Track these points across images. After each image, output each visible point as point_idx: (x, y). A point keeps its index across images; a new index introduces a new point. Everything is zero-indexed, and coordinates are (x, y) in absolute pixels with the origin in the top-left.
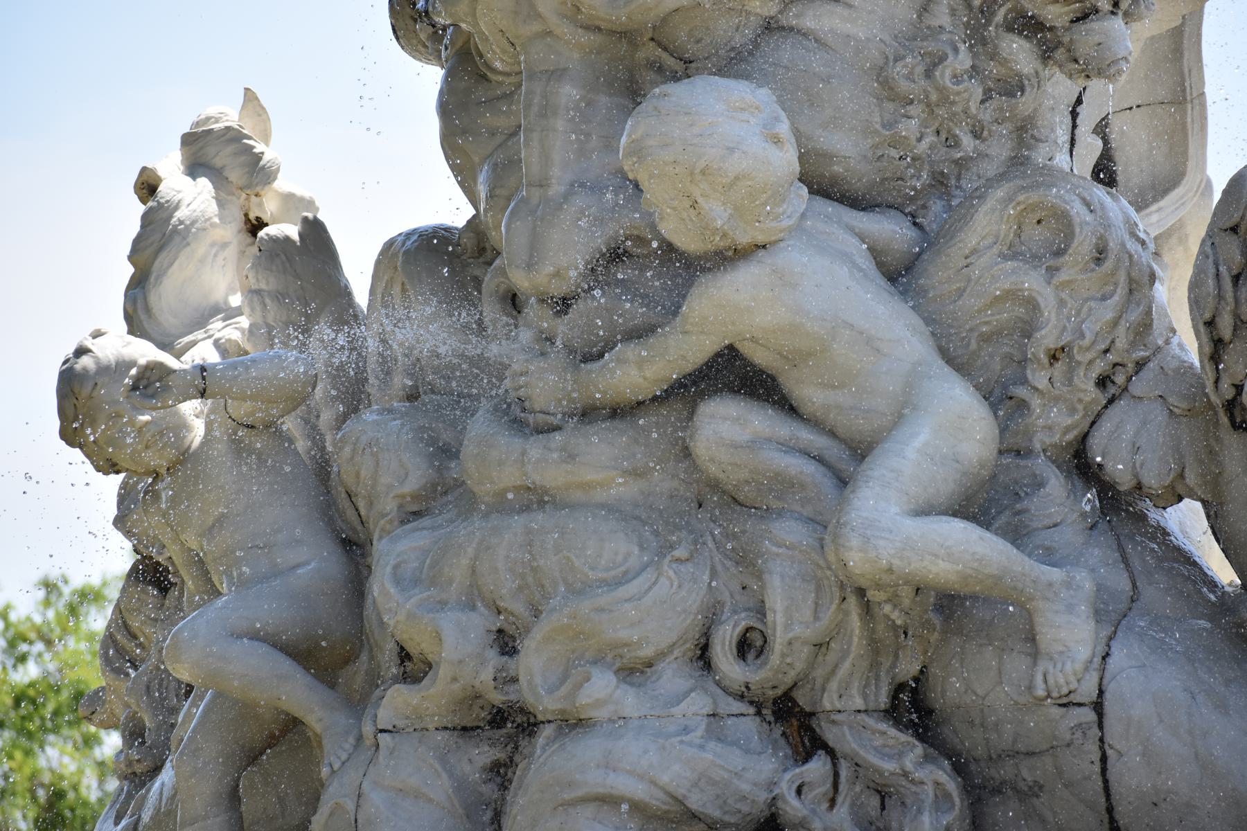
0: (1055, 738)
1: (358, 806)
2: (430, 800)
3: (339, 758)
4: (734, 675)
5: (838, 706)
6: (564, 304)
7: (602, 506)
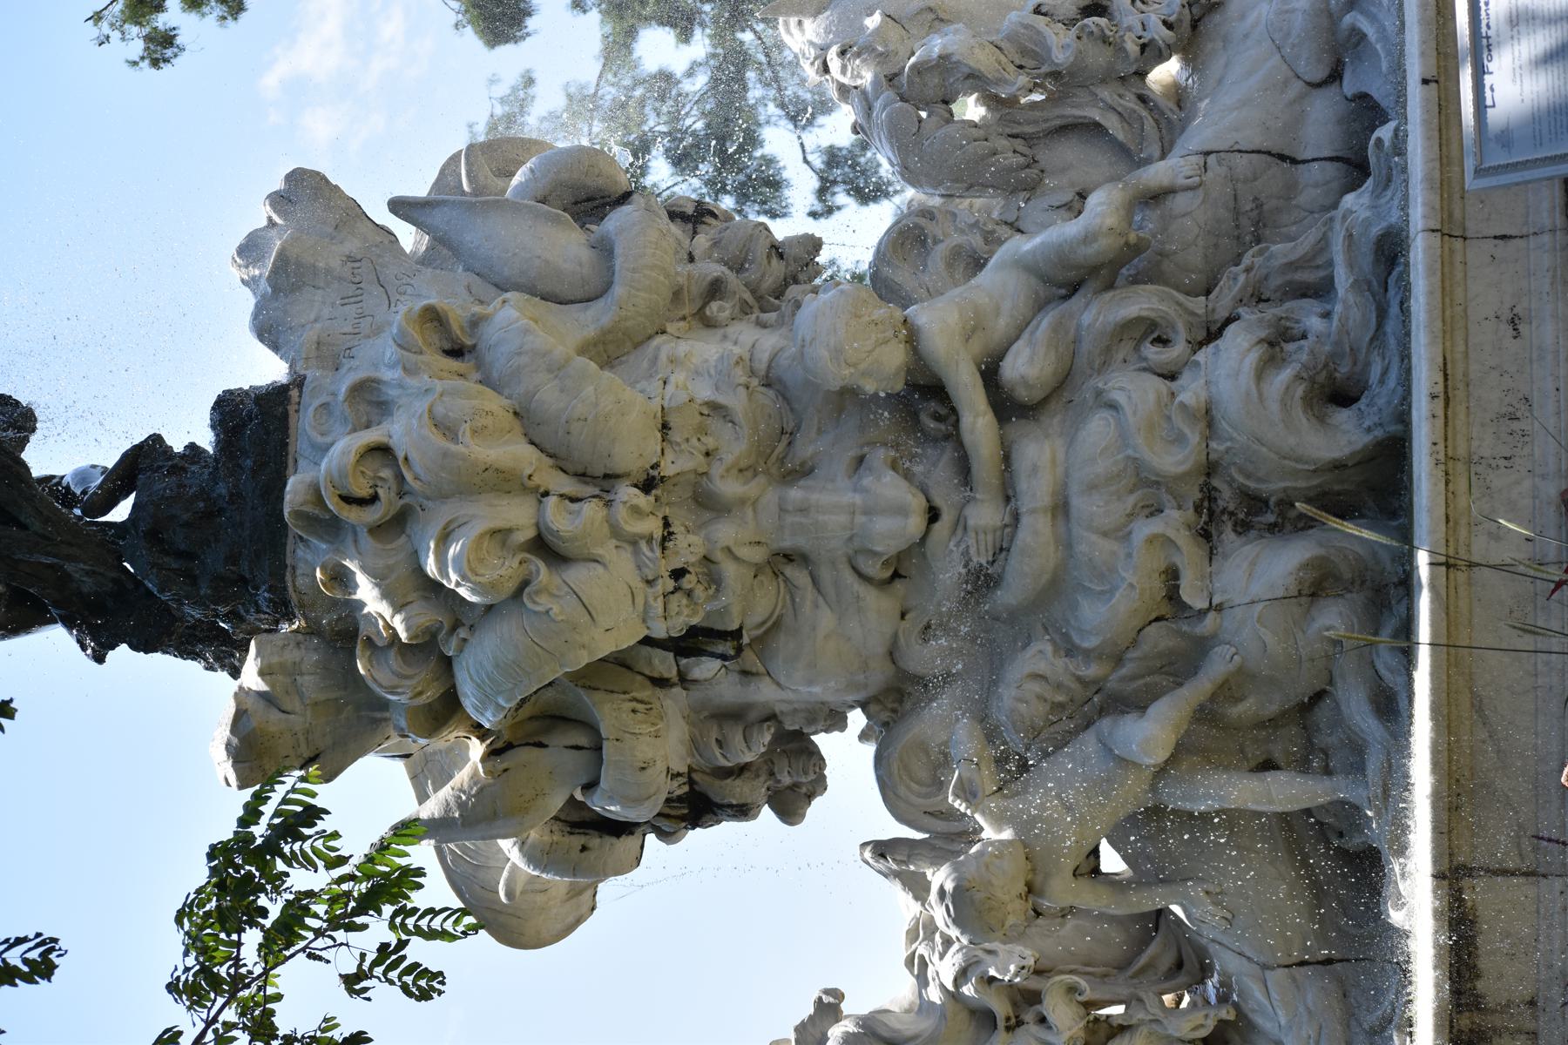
0: (1226, 177)
1: (1260, 601)
2: (1257, 556)
3: (1228, 650)
4: (1182, 348)
5: (1204, 305)
6: (933, 515)
7: (1067, 453)
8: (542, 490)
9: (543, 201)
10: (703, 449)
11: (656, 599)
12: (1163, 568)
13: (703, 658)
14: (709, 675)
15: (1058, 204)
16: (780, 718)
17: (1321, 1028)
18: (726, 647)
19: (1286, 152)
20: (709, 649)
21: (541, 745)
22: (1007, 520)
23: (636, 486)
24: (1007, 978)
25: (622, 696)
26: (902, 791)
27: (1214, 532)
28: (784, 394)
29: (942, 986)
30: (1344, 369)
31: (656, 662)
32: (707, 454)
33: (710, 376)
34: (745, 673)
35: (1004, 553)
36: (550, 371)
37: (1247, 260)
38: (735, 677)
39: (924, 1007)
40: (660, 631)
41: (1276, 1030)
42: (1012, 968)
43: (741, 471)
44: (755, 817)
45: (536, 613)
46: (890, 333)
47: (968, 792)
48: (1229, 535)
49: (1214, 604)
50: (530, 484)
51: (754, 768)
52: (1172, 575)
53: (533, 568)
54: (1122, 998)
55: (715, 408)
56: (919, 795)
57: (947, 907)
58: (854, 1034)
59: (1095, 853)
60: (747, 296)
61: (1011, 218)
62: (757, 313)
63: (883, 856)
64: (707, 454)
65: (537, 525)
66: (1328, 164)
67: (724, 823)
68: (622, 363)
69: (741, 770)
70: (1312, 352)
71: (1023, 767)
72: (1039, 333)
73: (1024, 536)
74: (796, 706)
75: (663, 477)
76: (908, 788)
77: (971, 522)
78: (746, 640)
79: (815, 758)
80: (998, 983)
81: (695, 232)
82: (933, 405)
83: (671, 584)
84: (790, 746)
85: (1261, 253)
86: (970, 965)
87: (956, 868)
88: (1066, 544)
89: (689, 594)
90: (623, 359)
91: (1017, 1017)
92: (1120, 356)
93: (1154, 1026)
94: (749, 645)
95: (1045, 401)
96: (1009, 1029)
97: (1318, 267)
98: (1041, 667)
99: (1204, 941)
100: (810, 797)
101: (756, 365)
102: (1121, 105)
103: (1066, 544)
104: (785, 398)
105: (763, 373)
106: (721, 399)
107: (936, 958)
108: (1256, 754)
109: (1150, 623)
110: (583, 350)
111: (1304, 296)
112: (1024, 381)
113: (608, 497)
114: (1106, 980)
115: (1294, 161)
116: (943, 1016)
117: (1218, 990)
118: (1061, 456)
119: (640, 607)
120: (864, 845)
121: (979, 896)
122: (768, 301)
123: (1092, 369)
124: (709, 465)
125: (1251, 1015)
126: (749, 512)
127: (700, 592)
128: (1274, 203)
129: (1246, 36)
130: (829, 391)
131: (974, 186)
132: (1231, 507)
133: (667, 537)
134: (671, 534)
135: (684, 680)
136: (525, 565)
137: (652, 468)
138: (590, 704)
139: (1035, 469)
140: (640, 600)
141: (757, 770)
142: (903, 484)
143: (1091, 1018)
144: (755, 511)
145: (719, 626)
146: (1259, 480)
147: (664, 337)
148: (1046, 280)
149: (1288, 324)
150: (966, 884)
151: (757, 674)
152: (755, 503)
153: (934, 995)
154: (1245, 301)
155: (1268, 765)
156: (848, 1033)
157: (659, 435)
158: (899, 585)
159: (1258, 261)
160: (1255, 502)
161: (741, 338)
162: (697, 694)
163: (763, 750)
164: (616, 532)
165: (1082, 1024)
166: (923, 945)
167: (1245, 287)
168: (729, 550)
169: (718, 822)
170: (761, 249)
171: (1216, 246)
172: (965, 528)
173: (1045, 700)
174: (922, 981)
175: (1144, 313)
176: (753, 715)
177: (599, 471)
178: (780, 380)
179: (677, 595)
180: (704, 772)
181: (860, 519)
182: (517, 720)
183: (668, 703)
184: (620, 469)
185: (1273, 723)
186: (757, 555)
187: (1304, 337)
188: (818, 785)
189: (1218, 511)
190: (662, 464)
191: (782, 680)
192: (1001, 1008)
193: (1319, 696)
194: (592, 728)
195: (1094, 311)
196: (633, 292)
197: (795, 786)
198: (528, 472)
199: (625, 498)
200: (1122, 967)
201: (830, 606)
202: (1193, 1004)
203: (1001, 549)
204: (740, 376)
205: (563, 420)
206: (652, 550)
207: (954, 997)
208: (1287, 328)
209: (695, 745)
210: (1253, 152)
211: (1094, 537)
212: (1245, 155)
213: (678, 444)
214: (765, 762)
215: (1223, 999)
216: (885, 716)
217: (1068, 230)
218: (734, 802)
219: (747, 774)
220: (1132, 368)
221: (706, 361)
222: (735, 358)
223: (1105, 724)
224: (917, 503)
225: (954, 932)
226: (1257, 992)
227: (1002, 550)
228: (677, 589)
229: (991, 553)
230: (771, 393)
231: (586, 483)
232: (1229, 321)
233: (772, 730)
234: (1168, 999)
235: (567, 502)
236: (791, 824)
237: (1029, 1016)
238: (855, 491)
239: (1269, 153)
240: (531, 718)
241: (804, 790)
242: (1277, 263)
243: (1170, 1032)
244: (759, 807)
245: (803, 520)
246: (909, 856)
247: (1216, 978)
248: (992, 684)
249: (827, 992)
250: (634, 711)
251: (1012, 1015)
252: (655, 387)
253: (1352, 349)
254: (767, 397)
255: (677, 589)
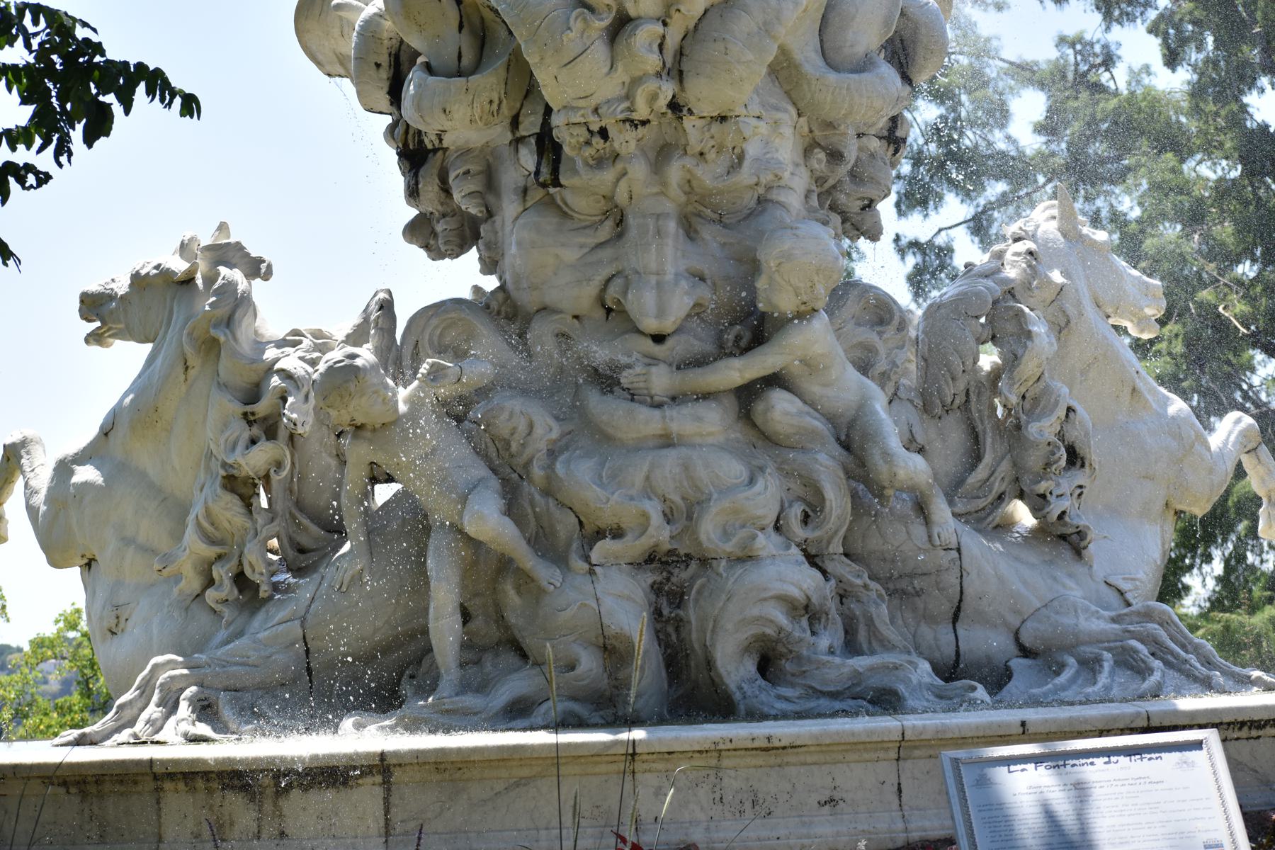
0: (940, 566)
2: (634, 601)
6: (659, 339)
7: (712, 445)
8: (668, 20)
9: (903, 14)
10: (705, 150)
11: (583, 116)
12: (622, 525)
13: (536, 157)
14: (522, 161)
15: (914, 431)
16: (489, 222)
17: (256, 666)
18: (545, 175)
19: (962, 614)
20: (544, 160)
21: (461, 27)
22: (656, 398)
23: (674, 96)
24: (286, 411)
25: (503, 92)
26: (434, 322)
27: (653, 566)
28: (751, 214)
29: (277, 360)
30: (788, 666)
31: (532, 118)
32: (701, 154)
33: (765, 154)
34: (525, 191)
35: (630, 397)
36: (765, 23)
37: (874, 585)
38: (521, 183)
39: (260, 346)
40: (556, 120)
41: (252, 630)
42: (294, 416)
43: (689, 181)
44: (409, 203)
45: (568, 19)
46: (805, 298)
47: (436, 374)
48: (650, 577)
49: (595, 568)
50: (673, 12)
51: (448, 201)
52: (617, 534)
53: (605, 15)
54: (274, 506)
55: (741, 157)
56: (431, 335)
57: (342, 361)
58: (236, 290)
59: (390, 479)
60: (831, 182)
61: (902, 394)
62: (817, 190)
63: (381, 308)
64: (701, 154)
65: (639, 18)
66: (954, 648)
67: (403, 178)
68: (773, 81)
69: (446, 191)
70: (801, 640)
71: (459, 419)
72: (808, 419)
73: (644, 413)
74: (500, 234)
75: (681, 118)
76: (436, 327)
77: (654, 369)
78: (552, 190)
79: (462, 249)
80: (281, 405)
81: (881, 138)
82: (747, 336)
83: (595, 128)
84: (467, 228)
85: (880, 596)
86: (295, 382)
87: (373, 367)
88: (638, 447)
89: (588, 143)
90: (777, 83)
91: (255, 421)
92: (792, 486)
93: (252, 532)
94: (548, 194)
95: (754, 425)
96: (245, 415)
97: (870, 643)
98: (539, 431)
99: (322, 570)
100: (426, 247)
101: (775, 191)
102: (996, 479)
103: (638, 447)
104: (750, 214)
105: (769, 197)
106: (747, 163)
107: (300, 354)
108: (474, 605)
109: (577, 517)
110: (783, 51)
111: (846, 632)
112: (769, 409)
113: (664, 76)
114: (288, 492)
115: (955, 619)
116: (253, 361)
117: (283, 582)
118: (710, 440)
119: (575, 104)
120: (389, 292)
121: (352, 387)
122: (827, 199)
123: (782, 463)
124: (693, 155)
125: (264, 610)
126: (655, 190)
127: (588, 152)
128: (921, 606)
129: (1055, 579)
130: (756, 250)
131: (926, 362)
132: (674, 579)
133: (635, 124)
134: (636, 126)
135: (518, 141)
136: (606, 9)
137: (689, 109)
138: (495, 66)
139: (699, 419)
140: (582, 103)
141: (447, 204)
142: (682, 314)
143: (257, 481)
144: (657, 194)
145: (562, 168)
146: (696, 601)
147: (795, 116)
148: (851, 425)
149: (823, 620)
150: (361, 375)
151: (524, 200)
152: (662, 193)
153: (270, 354)
154: (841, 585)
155: (466, 616)
156: (237, 285)
157: (715, 114)
158: (601, 313)
159: (874, 595)
160: (678, 598)
161: (796, 178)
162: (507, 152)
163: (463, 208)
164: (636, 82)
165: (251, 474)
166: (310, 343)
167: (852, 585)
168: (625, 174)
169: (404, 174)
170: (868, 191)
171: (884, 560)
172: (650, 365)
173: (512, 434)
174: (281, 344)
175: (828, 503)
176: (491, 199)
177: (685, 67)
178: (764, 210)
179: (587, 133)
180: (443, 160)
181: (653, 279)
182: (481, 8)
183: (499, 129)
184: (687, 84)
185: (500, 619)
186: (621, 196)
187: (814, 633)
188: (436, 253)
189: (670, 569)
190: (692, 117)
191: (521, 221)
192: (262, 408)
193: (524, 655)
194: (476, 68)
195: (828, 463)
196: (831, 90)
197: (434, 234)
198: (682, 8)
199: (664, 88)
200: (299, 505)
201: (581, 257)
202: (270, 563)
203: (633, 395)
204: (766, 178)
205: (727, 36)
206: (622, 112)
207: (270, 370)
208: (819, 620)
209: (466, 152)
210: (961, 587)
211: (645, 468)
212: (959, 581)
213: (709, 130)
214: (454, 210)
215: (276, 587)
216: (494, 305)
217: (894, 441)
218: (420, 186)
219: (443, 195)
220: (783, 495)
221: (777, 151)
222: (780, 174)
223: (495, 483)
224: (668, 325)
225: (322, 367)
226: (281, 615)
227: (632, 396)
228: (591, 132)
229: (629, 386)
230: (753, 204)
231: (675, 56)
232: (824, 572)
233: (480, 215)
234: (274, 543)
235: (659, 41)
236: (404, 233)
237: (256, 430)
238: (676, 275)
239: (961, 600)
240: (482, 18)
241: (432, 242)
242: (873, 609)
243: (248, 545)
244: (417, 206)
245: (651, 233)
246: (381, 329)
247: (292, 580)
248: (523, 390)
249: (269, 267)
250: (491, 102)
251: (257, 417)
252: (756, 109)
253: (804, 672)
254: (749, 200)
255: (591, 132)
